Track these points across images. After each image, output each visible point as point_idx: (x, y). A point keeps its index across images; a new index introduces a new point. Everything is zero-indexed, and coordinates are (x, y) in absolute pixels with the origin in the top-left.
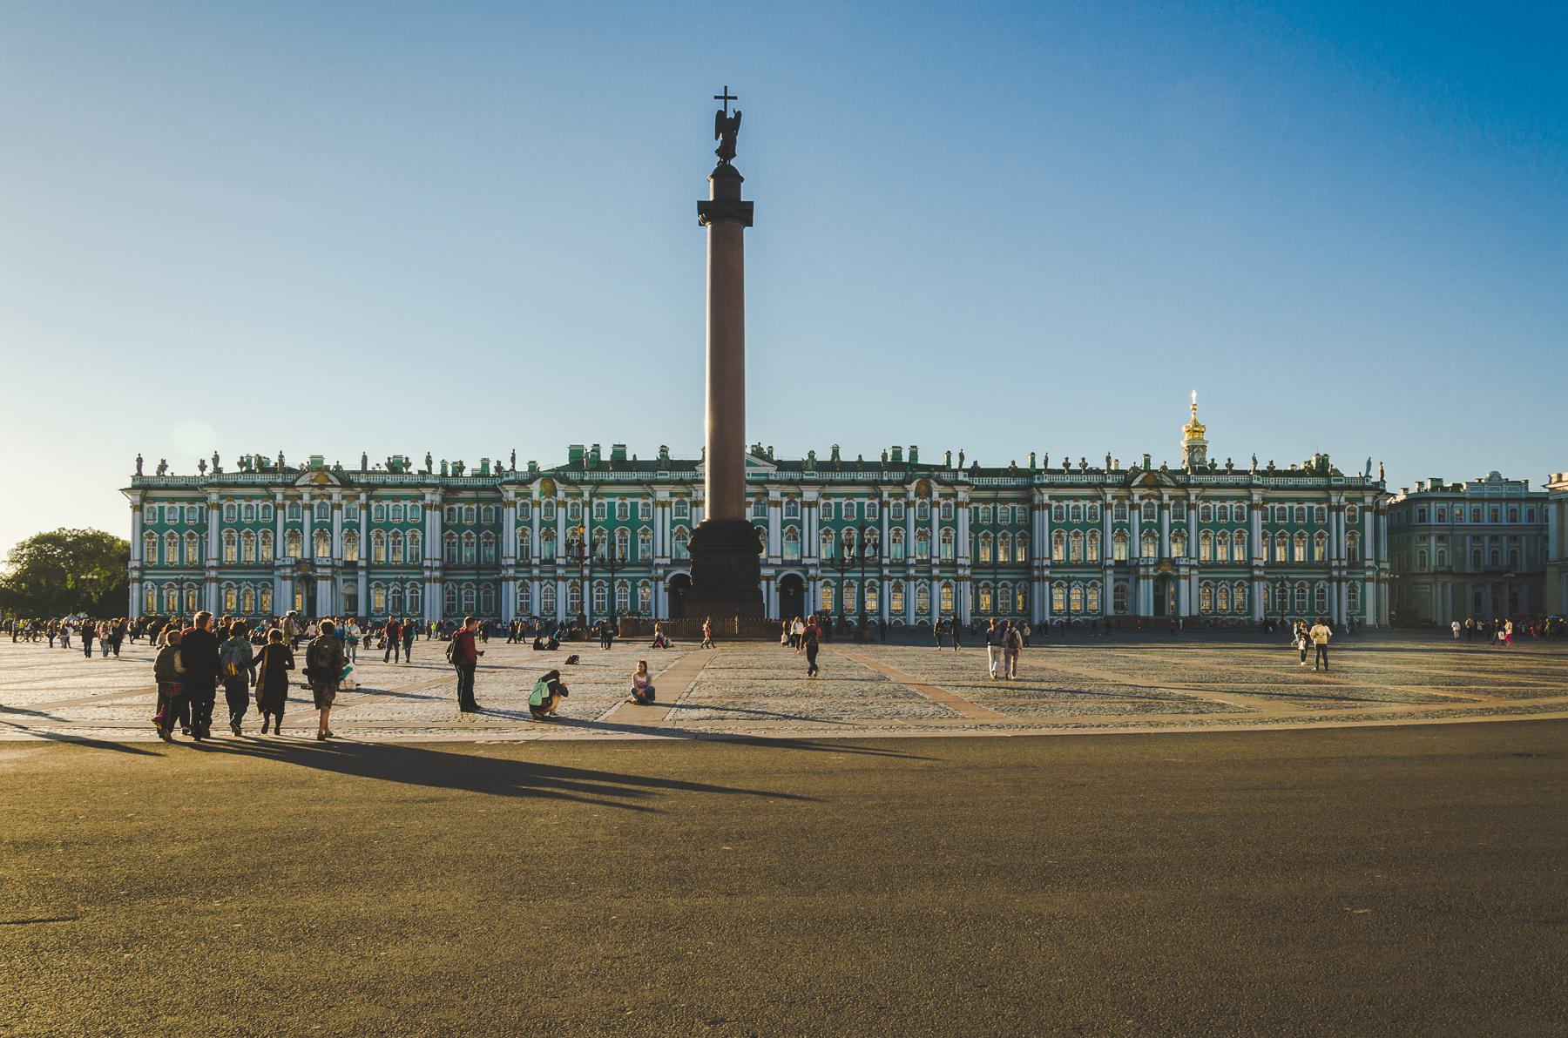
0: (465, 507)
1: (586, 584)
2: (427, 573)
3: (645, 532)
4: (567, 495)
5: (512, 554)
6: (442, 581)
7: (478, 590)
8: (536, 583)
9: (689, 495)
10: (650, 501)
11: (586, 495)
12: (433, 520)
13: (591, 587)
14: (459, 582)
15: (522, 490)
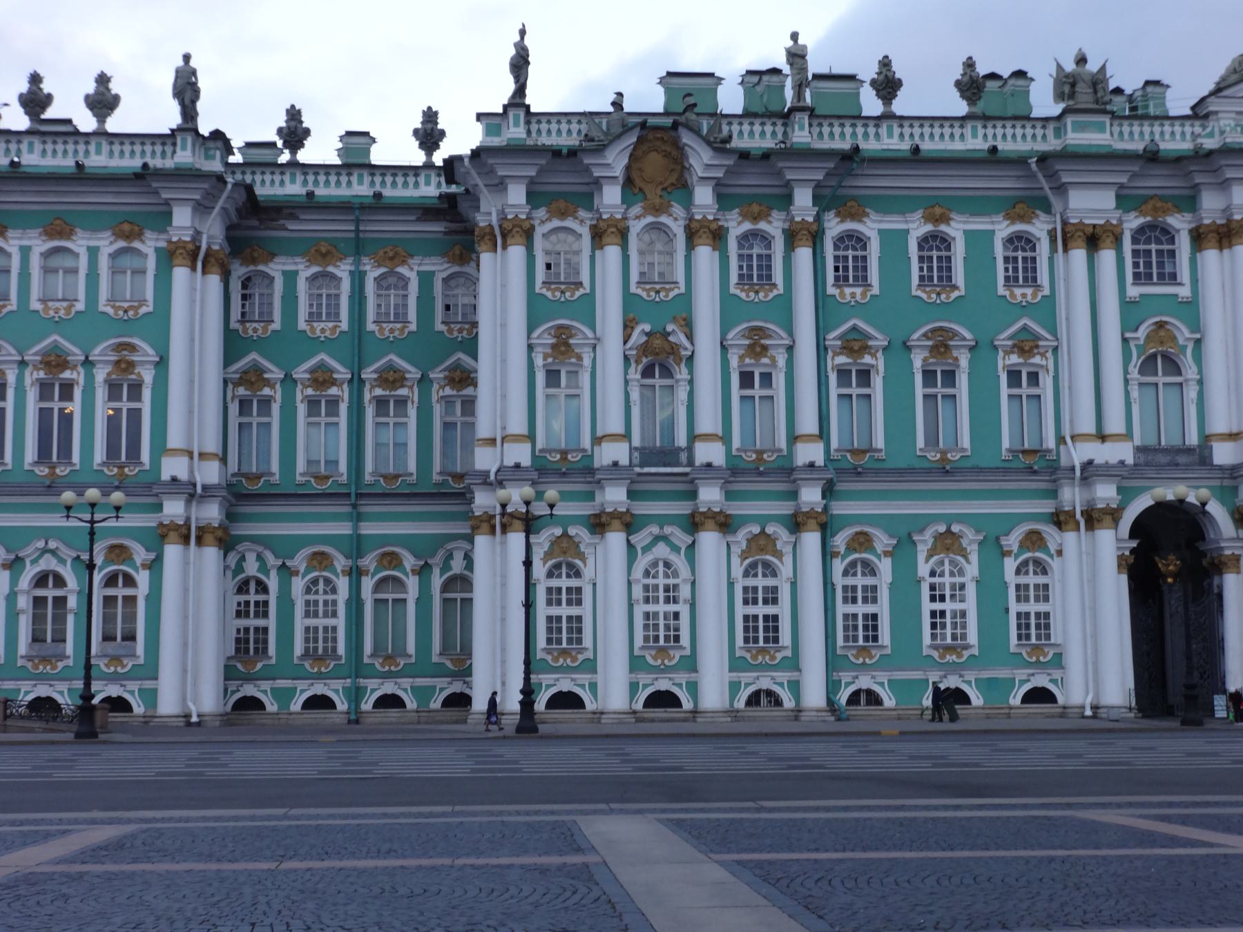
0: (305, 272)
1: (811, 540)
2: (174, 509)
3: (1026, 345)
4: (724, 199)
5: (518, 425)
6: (227, 543)
7: (356, 574)
8: (616, 539)
9: (1190, 202)
10: (1039, 228)
11: (803, 199)
12: (196, 303)
13: (827, 555)
14: (284, 547)
15: (564, 180)
